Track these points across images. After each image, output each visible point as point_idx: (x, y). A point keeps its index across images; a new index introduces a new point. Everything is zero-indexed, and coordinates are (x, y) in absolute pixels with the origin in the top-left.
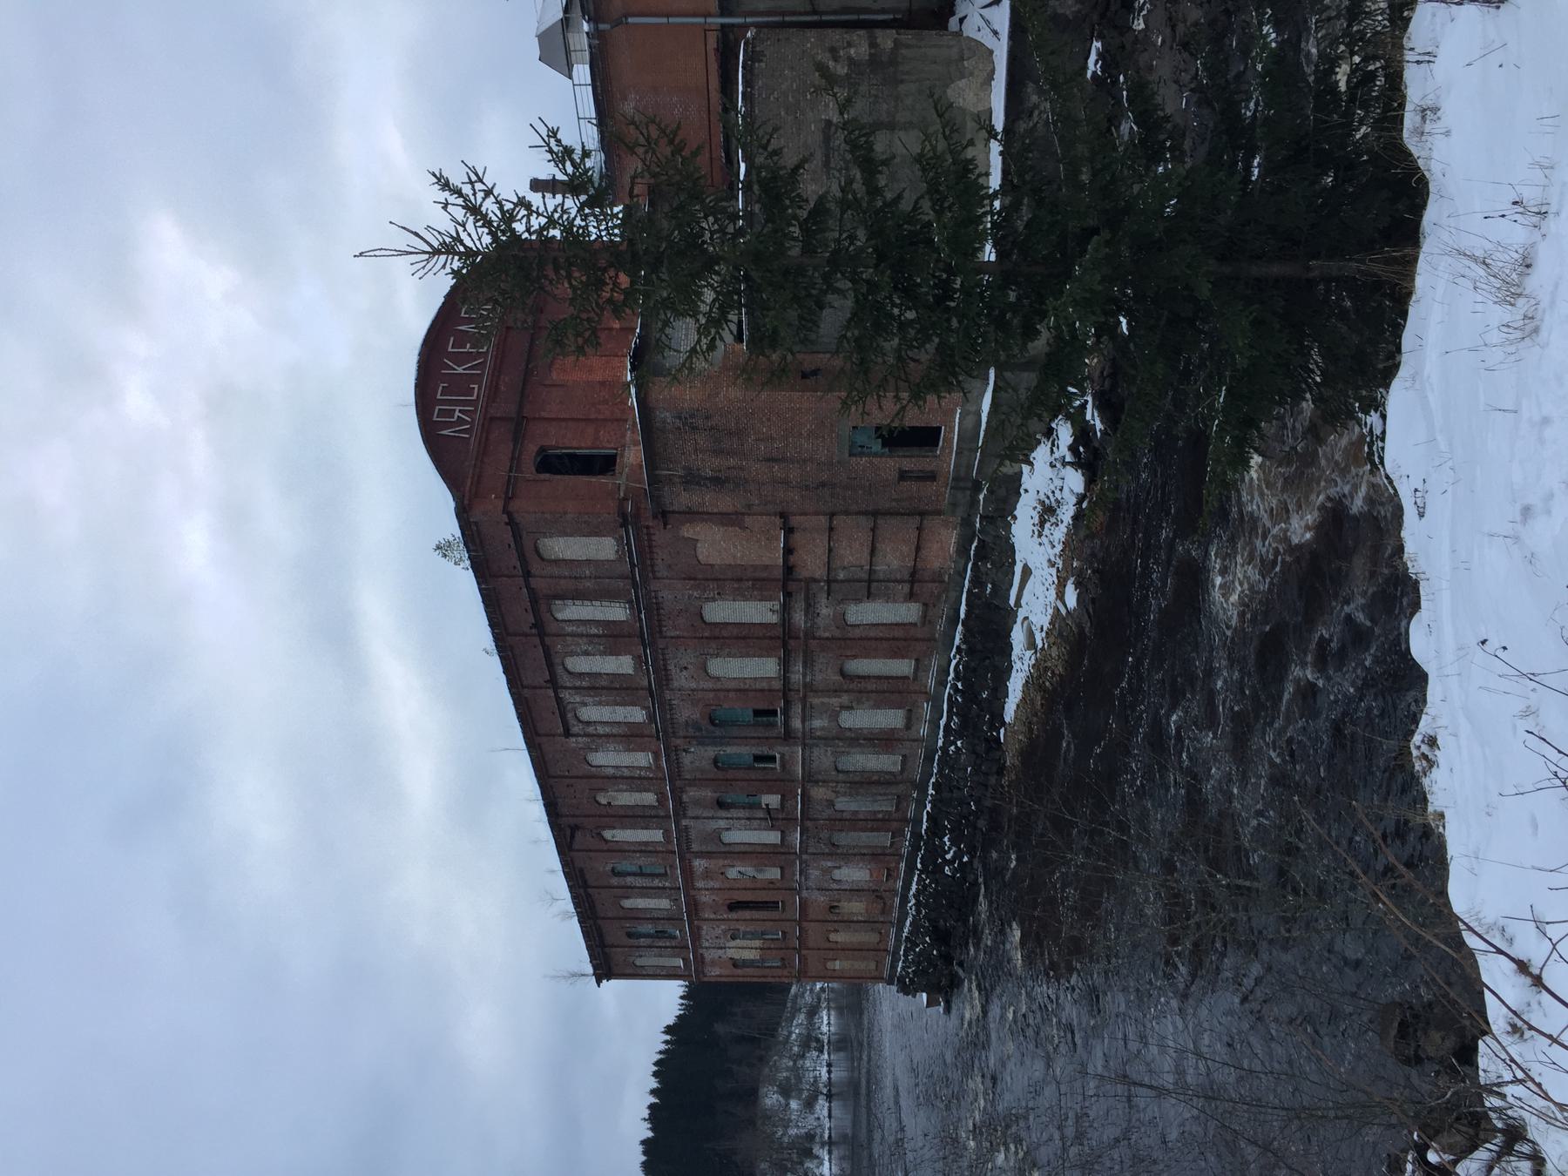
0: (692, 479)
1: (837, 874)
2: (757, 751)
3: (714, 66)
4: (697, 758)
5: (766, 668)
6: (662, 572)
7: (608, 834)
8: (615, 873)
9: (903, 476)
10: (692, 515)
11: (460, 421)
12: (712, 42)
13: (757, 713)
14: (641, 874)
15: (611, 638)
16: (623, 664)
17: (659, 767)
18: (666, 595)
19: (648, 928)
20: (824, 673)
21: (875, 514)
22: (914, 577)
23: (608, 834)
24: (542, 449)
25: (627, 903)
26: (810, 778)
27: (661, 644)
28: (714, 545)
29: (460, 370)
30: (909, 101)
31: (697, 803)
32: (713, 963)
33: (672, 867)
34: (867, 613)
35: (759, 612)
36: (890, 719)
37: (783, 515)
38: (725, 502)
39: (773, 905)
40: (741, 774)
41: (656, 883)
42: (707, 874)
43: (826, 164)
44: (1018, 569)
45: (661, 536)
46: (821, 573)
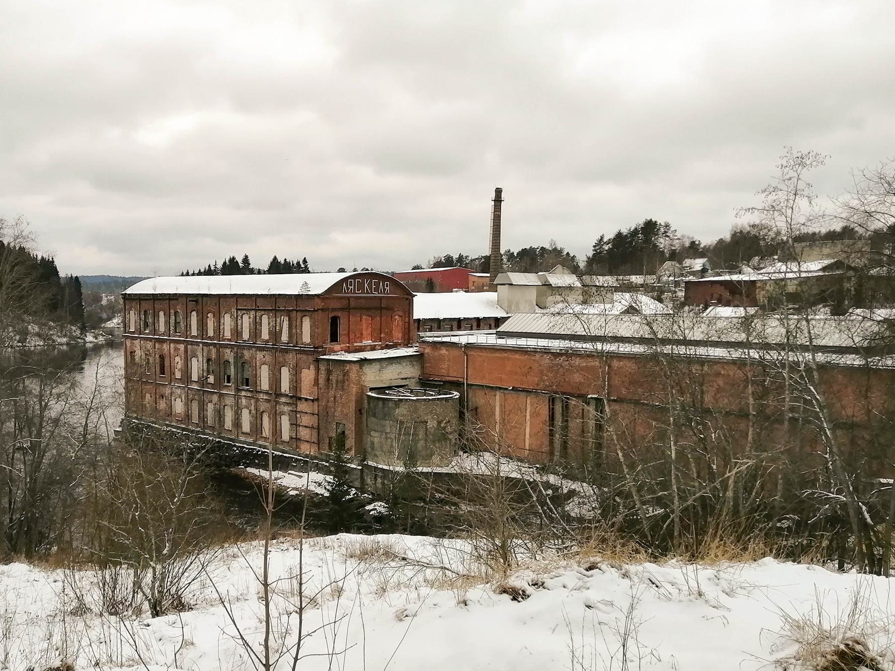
0: (329, 372)
1: (178, 400)
2: (232, 376)
3: (455, 379)
4: (229, 355)
5: (265, 385)
6: (299, 356)
7: (194, 313)
8: (176, 313)
9: (330, 438)
10: (318, 370)
11: (348, 289)
12: (461, 380)
13: (247, 380)
14: (176, 323)
15: (275, 334)
16: (265, 335)
17: (224, 340)
18: (291, 356)
19: (150, 320)
20: (263, 406)
21: (318, 429)
22: (298, 439)
23: (194, 313)
24: (339, 317)
25: (161, 314)
26: (221, 396)
27: (274, 351)
28: (308, 375)
31: (209, 351)
32: (132, 344)
33: (180, 336)
34: (285, 422)
35: (285, 387)
36: (246, 427)
37: (317, 400)
38: (322, 381)
39: (162, 372)
40: (222, 370)
41: (172, 328)
42: (176, 349)
44: (301, 474)
45: (311, 358)
46: (299, 409)
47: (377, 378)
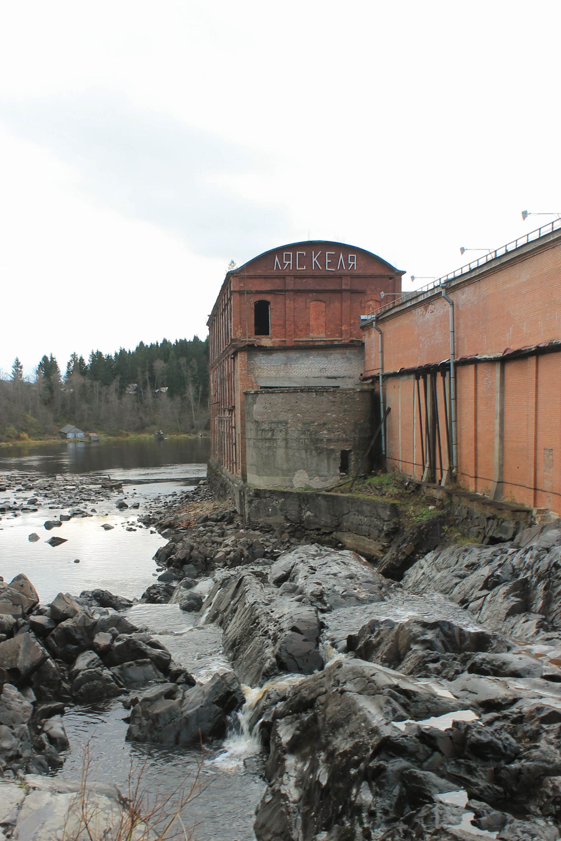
29: (314, 260)
30: (297, 454)
43: (273, 422)
47: (282, 374)
